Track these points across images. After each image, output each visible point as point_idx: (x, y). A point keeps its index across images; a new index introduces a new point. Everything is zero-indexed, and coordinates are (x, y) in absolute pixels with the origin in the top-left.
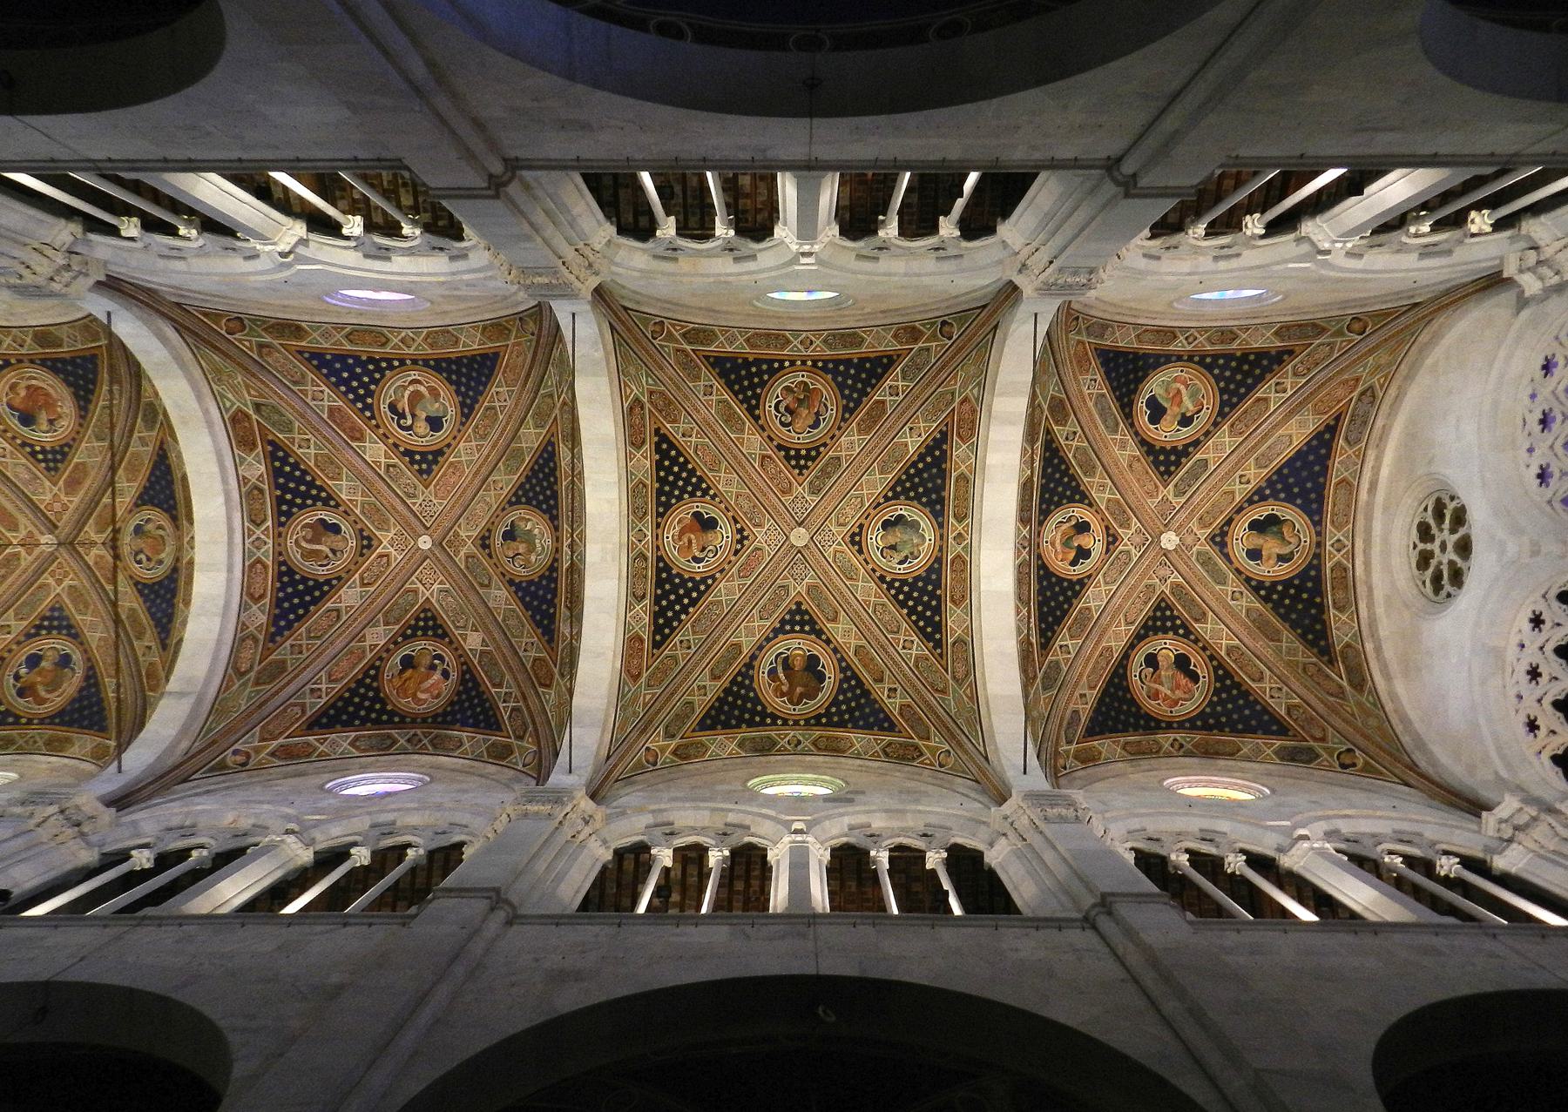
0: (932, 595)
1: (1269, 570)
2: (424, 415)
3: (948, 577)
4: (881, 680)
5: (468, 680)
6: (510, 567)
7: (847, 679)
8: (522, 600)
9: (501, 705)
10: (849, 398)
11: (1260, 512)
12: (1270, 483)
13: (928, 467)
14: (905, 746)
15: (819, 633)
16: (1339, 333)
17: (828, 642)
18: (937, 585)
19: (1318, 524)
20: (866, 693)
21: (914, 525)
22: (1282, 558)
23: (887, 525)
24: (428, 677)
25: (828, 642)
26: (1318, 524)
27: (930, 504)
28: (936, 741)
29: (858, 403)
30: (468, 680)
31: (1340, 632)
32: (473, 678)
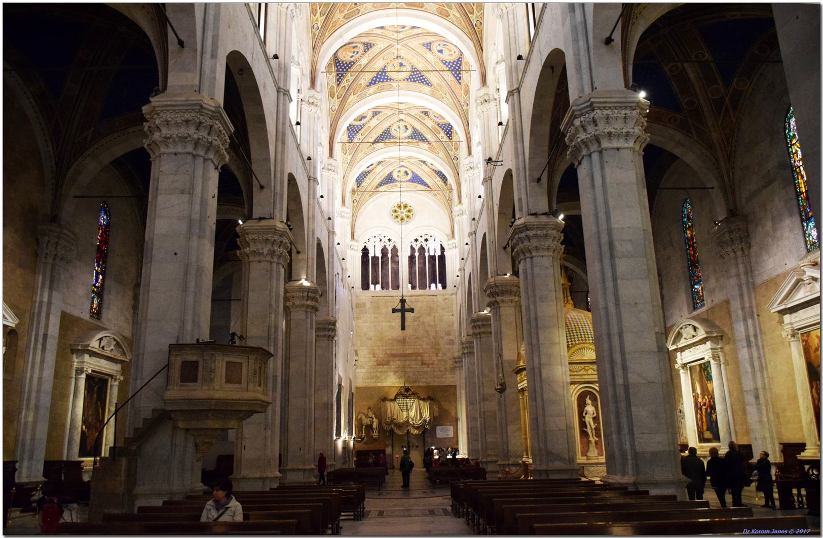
1: (395, 175)
2: (443, 49)
5: (351, 64)
6: (391, 65)
7: (361, 126)
9: (345, 80)
11: (409, 172)
12: (416, 175)
15: (373, 117)
20: (358, 132)
21: (406, 132)
23: (406, 126)
24: (351, 52)
27: (412, 136)
28: (350, 157)
29: (440, 127)
30: (351, 64)
31: (381, 189)
32: (352, 66)
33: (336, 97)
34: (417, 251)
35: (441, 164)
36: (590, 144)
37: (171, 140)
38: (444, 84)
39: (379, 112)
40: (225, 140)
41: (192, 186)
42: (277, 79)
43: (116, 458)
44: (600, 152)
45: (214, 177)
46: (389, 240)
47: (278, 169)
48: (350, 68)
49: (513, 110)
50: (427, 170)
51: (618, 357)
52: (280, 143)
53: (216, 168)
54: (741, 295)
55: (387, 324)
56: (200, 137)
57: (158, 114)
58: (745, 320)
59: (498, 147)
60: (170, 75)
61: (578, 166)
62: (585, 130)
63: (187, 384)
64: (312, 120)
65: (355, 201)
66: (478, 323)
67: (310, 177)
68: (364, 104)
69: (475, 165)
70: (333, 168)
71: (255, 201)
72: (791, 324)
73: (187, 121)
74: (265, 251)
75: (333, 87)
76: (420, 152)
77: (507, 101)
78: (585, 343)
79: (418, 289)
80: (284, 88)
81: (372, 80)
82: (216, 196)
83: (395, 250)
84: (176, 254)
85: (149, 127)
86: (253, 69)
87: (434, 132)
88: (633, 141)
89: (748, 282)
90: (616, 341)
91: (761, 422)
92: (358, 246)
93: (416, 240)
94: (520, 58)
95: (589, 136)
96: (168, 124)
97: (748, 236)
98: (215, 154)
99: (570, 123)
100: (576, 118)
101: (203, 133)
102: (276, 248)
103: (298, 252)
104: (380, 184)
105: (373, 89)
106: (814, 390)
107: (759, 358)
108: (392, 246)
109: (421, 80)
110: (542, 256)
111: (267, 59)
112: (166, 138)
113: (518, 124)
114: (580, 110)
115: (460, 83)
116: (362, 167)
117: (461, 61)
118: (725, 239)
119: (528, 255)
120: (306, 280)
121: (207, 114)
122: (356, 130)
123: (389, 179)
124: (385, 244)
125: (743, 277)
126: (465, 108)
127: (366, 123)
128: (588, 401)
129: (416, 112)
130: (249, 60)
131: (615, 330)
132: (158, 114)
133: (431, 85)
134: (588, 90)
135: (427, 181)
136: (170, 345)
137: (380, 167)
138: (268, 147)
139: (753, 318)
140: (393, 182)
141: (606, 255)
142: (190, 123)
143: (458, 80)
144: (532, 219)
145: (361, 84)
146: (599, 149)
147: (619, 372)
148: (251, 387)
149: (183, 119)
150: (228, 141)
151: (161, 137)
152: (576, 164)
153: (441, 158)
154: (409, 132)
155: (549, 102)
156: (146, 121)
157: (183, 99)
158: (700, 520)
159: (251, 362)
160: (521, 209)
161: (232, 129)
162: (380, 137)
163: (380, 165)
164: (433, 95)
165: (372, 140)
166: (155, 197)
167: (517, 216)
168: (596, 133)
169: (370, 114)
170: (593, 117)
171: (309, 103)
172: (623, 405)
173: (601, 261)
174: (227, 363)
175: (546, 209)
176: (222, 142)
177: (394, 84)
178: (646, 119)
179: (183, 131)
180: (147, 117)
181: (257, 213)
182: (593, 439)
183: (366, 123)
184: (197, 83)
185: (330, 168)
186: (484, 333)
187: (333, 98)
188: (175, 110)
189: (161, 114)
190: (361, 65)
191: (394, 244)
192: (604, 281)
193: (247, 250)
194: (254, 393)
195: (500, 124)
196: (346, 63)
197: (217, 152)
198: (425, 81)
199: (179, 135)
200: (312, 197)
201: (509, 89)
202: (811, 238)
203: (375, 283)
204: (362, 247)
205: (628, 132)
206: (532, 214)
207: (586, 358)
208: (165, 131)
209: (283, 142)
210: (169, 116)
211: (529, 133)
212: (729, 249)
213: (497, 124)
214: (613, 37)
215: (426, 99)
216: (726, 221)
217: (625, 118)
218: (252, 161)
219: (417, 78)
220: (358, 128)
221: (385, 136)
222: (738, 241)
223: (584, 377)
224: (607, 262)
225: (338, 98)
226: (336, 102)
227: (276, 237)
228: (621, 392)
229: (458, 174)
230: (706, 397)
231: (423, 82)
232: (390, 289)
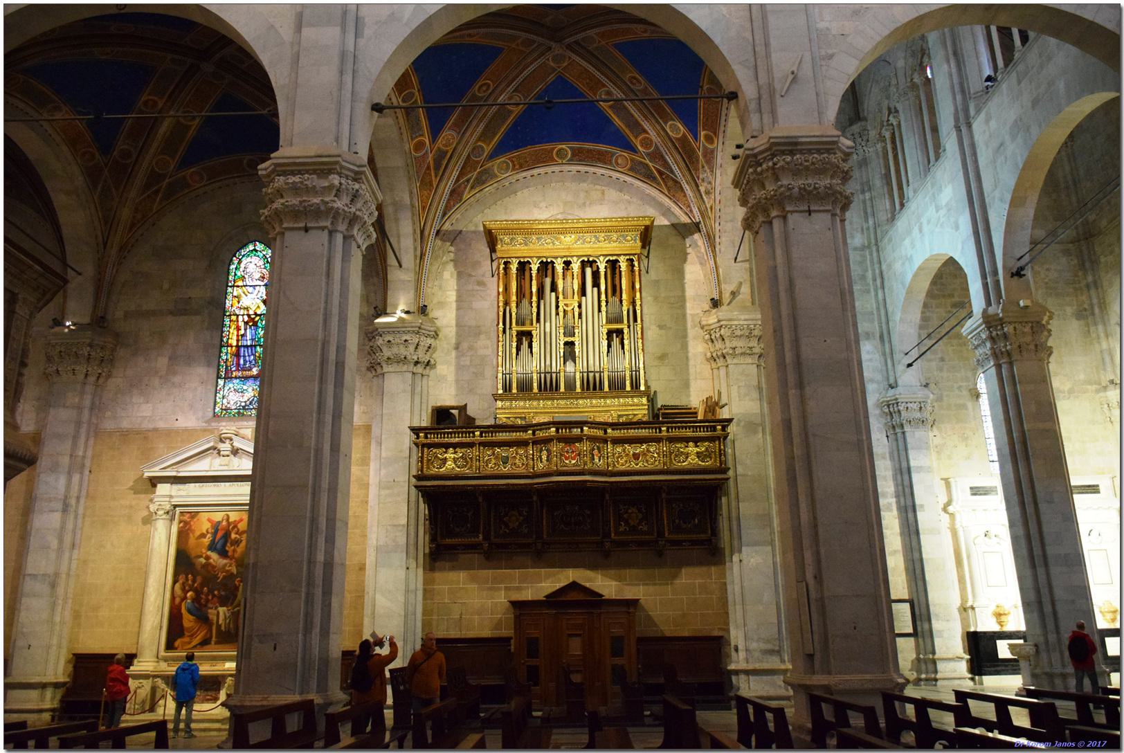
54: (75, 438)
72: (171, 497)
89: (89, 423)
91: (51, 622)
97: (111, 361)
106: (178, 586)
107: (74, 531)
114: (342, 167)
118: (81, 352)
125: (86, 413)
139: (82, 473)
146: (346, 233)
168: (358, 213)
170: (357, 191)
172: (318, 592)
173: (322, 380)
202: (225, 401)
212: (81, 369)
222: (97, 362)
224: (330, 388)
228: (319, 571)
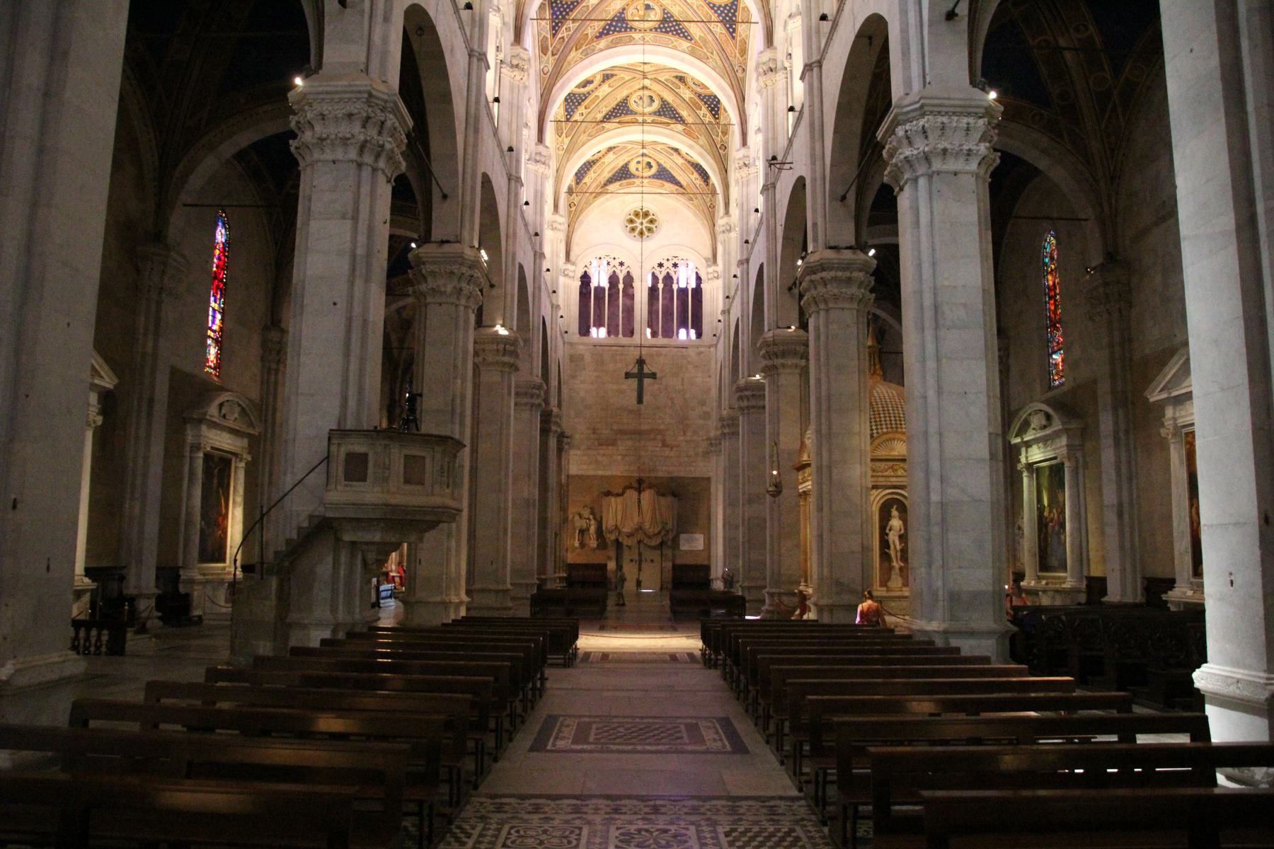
0: (622, 113)
1: (632, 167)
3: (629, 118)
4: (586, 108)
7: (584, 95)
8: (616, 16)
9: (564, 28)
10: (704, 97)
11: (653, 164)
13: (674, 115)
14: (562, 129)
16: (711, 200)
17: (600, 85)
18: (626, 114)
19: (650, 177)
20: (579, 104)
21: (650, 105)
22: (637, 169)
23: (651, 97)
25: (600, 85)
26: (650, 177)
27: (659, 111)
28: (567, 141)
29: (702, 100)
31: (611, 187)
32: (575, 7)
33: (550, 52)
34: (661, 281)
35: (700, 155)
36: (917, 166)
37: (329, 141)
38: (710, 38)
39: (612, 75)
40: (402, 141)
41: (356, 210)
42: (469, 37)
43: (265, 576)
44: (930, 177)
45: (385, 191)
46: (621, 264)
47: (469, 171)
48: (571, 10)
49: (810, 90)
50: (680, 161)
51: (935, 465)
52: (471, 132)
53: (389, 181)
55: (615, 387)
56: (369, 138)
57: (310, 105)
58: (1115, 409)
59: (786, 143)
60: (326, 48)
61: (898, 193)
62: (910, 143)
63: (355, 483)
64: (516, 91)
65: (572, 205)
66: (747, 393)
67: (510, 175)
68: (591, 64)
69: (751, 161)
70: (543, 160)
71: (434, 215)
73: (350, 116)
74: (449, 289)
75: (547, 38)
76: (667, 137)
77: (802, 78)
78: (897, 432)
79: (660, 336)
80: (479, 50)
81: (604, 29)
82: (388, 221)
83: (629, 279)
84: (335, 304)
85: (298, 122)
86: (437, 28)
87: (693, 107)
88: (978, 162)
90: (934, 445)
92: (574, 271)
93: (661, 265)
94: (824, 18)
95: (915, 152)
96: (324, 119)
98: (388, 161)
99: (891, 131)
100: (898, 124)
101: (372, 132)
102: (464, 285)
103: (492, 286)
104: (611, 181)
105: (603, 42)
108: (625, 272)
109: (676, 30)
110: (843, 309)
111: (456, 10)
112: (322, 139)
113: (817, 114)
115: (733, 38)
116: (586, 154)
117: (736, 5)
119: (822, 306)
120: (502, 326)
121: (377, 104)
122: (577, 101)
123: (623, 174)
124: (614, 269)
126: (740, 74)
127: (593, 91)
128: (895, 513)
129: (667, 77)
130: (432, 13)
131: (932, 429)
132: (310, 105)
133: (691, 40)
134: (916, 85)
135: (680, 179)
136: (331, 430)
137: (611, 156)
138: (455, 138)
140: (630, 178)
141: (929, 323)
142: (353, 118)
143: (731, 33)
144: (830, 254)
145: (587, 34)
146: (930, 171)
147: (935, 484)
148: (437, 489)
149: (344, 111)
150: (406, 141)
151: (313, 137)
152: (897, 189)
153: (702, 146)
154: (656, 105)
155: (863, 86)
156: (294, 114)
157: (345, 83)
158: (1009, 695)
159: (438, 456)
160: (815, 240)
161: (411, 123)
162: (612, 112)
163: (611, 153)
164: (692, 53)
165: (600, 117)
166: (307, 224)
167: (810, 249)
169: (599, 78)
170: (923, 126)
171: (512, 66)
174: (406, 456)
175: (853, 242)
176: (394, 144)
177: (636, 36)
178: (996, 131)
179: (344, 129)
180: (295, 107)
181: (437, 234)
182: (896, 564)
183: (593, 91)
184: (363, 59)
185: (538, 158)
186: (754, 407)
187: (545, 55)
188: (332, 99)
189: (315, 105)
190: (588, 6)
191: (628, 269)
192: (924, 361)
193: (423, 287)
194: (440, 498)
195: (791, 109)
196: (566, 3)
197: (390, 158)
198: (682, 32)
199: (340, 135)
200: (512, 205)
201: (807, 61)
203: (599, 324)
204: (580, 273)
205: (970, 150)
206: (831, 248)
207: (896, 453)
208: (318, 128)
209: (476, 131)
210: (325, 109)
211: (832, 129)
213: (786, 111)
214: (957, 11)
215: (683, 60)
216: (1101, 268)
217: (968, 129)
218: (432, 157)
219: (670, 27)
220: (581, 98)
221: (620, 111)
223: (892, 479)
225: (553, 55)
226: (550, 61)
227: (464, 269)
229: (726, 171)
230: (1055, 511)
231: (678, 34)
232: (620, 336)
